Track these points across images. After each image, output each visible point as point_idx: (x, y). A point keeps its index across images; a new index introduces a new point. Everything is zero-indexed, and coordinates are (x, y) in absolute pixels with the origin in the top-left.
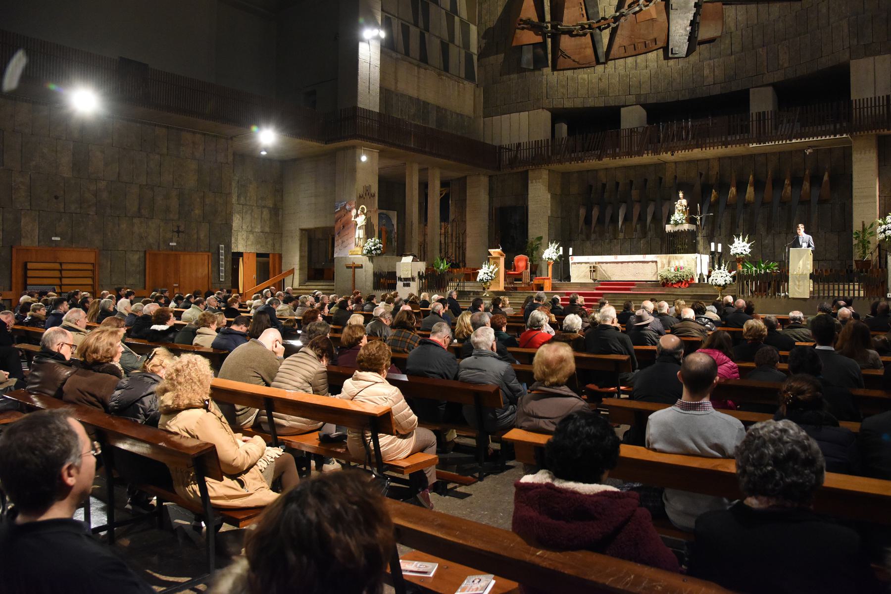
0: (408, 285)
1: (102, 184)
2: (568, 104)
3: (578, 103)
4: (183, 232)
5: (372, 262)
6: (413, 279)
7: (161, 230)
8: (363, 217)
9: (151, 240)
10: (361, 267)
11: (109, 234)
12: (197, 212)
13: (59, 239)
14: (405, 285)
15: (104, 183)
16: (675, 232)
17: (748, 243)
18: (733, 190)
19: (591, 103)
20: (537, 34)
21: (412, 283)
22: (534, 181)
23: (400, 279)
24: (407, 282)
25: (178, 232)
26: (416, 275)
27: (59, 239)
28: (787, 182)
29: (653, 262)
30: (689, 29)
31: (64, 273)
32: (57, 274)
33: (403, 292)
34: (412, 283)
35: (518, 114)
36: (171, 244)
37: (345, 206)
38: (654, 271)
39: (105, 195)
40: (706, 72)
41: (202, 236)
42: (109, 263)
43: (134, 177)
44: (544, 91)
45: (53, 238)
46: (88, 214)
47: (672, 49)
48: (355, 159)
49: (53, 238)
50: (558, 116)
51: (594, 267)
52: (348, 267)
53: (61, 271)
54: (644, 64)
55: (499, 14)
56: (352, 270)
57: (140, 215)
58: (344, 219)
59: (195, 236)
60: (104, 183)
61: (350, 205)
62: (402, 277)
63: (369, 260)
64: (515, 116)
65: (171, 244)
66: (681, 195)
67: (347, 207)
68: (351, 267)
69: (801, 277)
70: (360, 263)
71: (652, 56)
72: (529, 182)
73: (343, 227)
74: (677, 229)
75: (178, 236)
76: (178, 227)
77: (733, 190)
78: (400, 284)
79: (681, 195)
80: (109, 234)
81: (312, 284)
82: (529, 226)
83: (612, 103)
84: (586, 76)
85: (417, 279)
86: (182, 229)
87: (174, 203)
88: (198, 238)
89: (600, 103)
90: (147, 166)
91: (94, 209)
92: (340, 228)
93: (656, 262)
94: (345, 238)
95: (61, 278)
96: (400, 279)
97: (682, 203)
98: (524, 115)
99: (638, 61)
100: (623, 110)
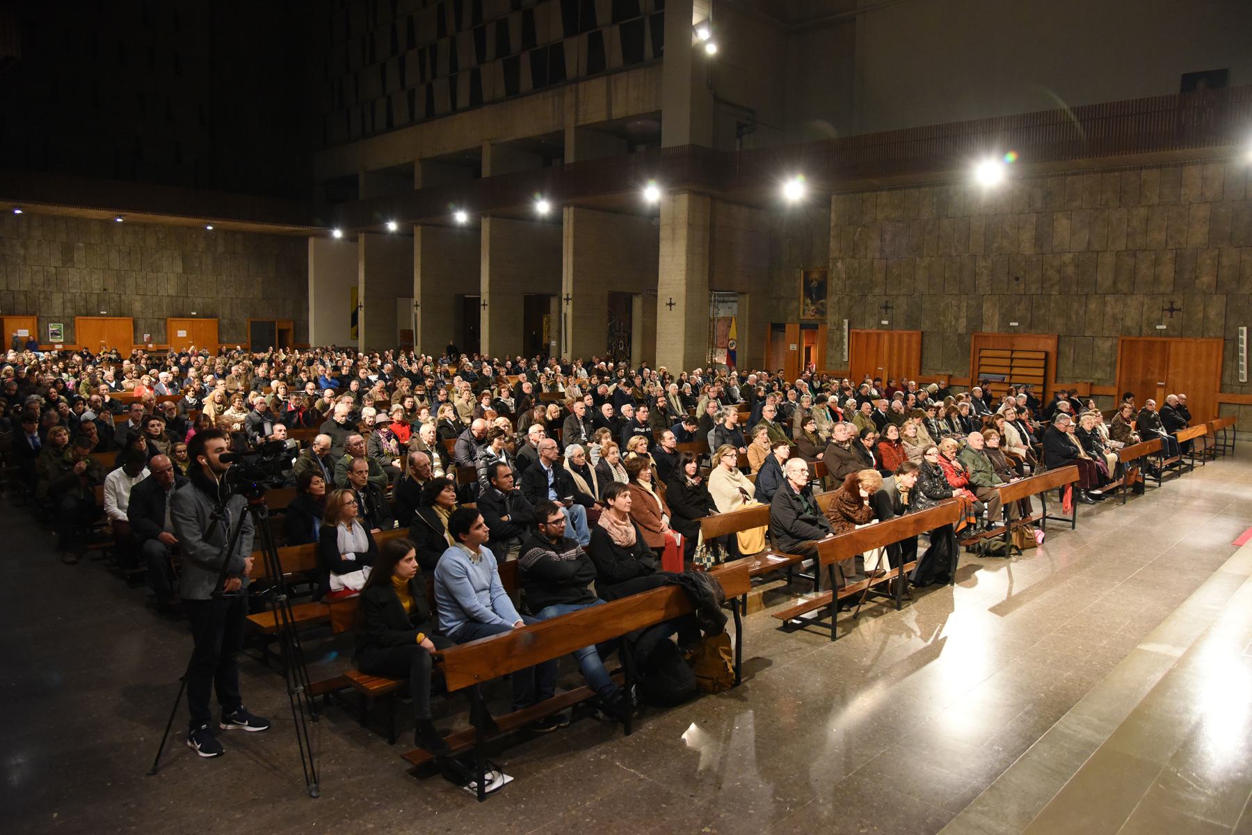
1: (1067, 258)
4: (1180, 310)
7: (1145, 308)
9: (1129, 323)
11: (1074, 317)
12: (1205, 279)
13: (1017, 324)
15: (1070, 255)
25: (1172, 310)
27: (1017, 324)
31: (1015, 363)
32: (1007, 362)
36: (1158, 327)
39: (1070, 270)
41: (1212, 313)
42: (1072, 351)
43: (1110, 243)
45: (1011, 324)
46: (1050, 295)
49: (1011, 324)
53: (1012, 359)
57: (1114, 291)
59: (1200, 315)
60: (1070, 255)
65: (1158, 327)
75: (1172, 315)
76: (1172, 303)
80: (1074, 317)
86: (1178, 304)
87: (1167, 271)
88: (1206, 317)
90: (1128, 226)
91: (1057, 288)
95: (1011, 367)
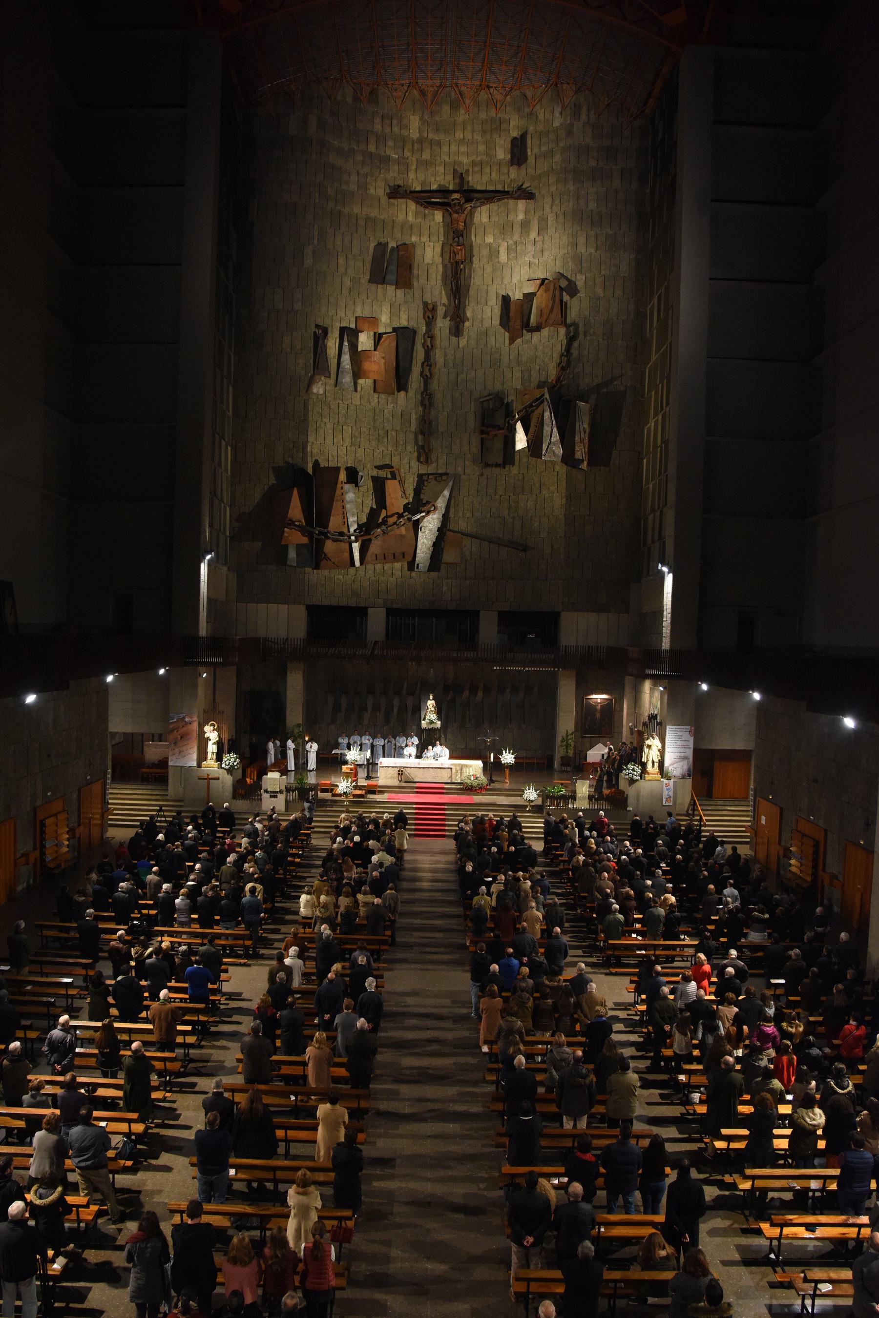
0: (276, 797)
2: (326, 602)
3: (334, 602)
5: (231, 775)
6: (281, 792)
8: (216, 733)
10: (218, 779)
14: (271, 797)
16: (429, 730)
17: (513, 754)
18: (466, 693)
19: (344, 602)
20: (303, 535)
21: (279, 795)
22: (294, 672)
23: (266, 791)
24: (274, 794)
26: (284, 788)
28: (508, 691)
29: (448, 768)
30: (431, 549)
33: (267, 803)
34: (279, 795)
35: (276, 605)
37: (184, 718)
38: (449, 776)
40: (445, 589)
44: (306, 588)
47: (418, 565)
48: (200, 675)
50: (312, 610)
51: (402, 771)
52: (199, 779)
54: (390, 572)
55: (256, 501)
56: (206, 781)
58: (181, 731)
61: (191, 718)
62: (269, 790)
63: (228, 773)
64: (273, 607)
66: (431, 697)
67: (187, 719)
68: (206, 779)
69: (583, 798)
70: (216, 776)
71: (397, 565)
72: (288, 672)
73: (181, 737)
74: (431, 726)
77: (466, 693)
78: (265, 796)
79: (431, 697)
81: (127, 786)
82: (288, 713)
83: (363, 605)
84: (341, 577)
85: (284, 792)
89: (352, 603)
92: (177, 738)
93: (451, 769)
94: (184, 748)
96: (266, 791)
97: (431, 703)
98: (283, 608)
99: (385, 568)
100: (369, 609)
